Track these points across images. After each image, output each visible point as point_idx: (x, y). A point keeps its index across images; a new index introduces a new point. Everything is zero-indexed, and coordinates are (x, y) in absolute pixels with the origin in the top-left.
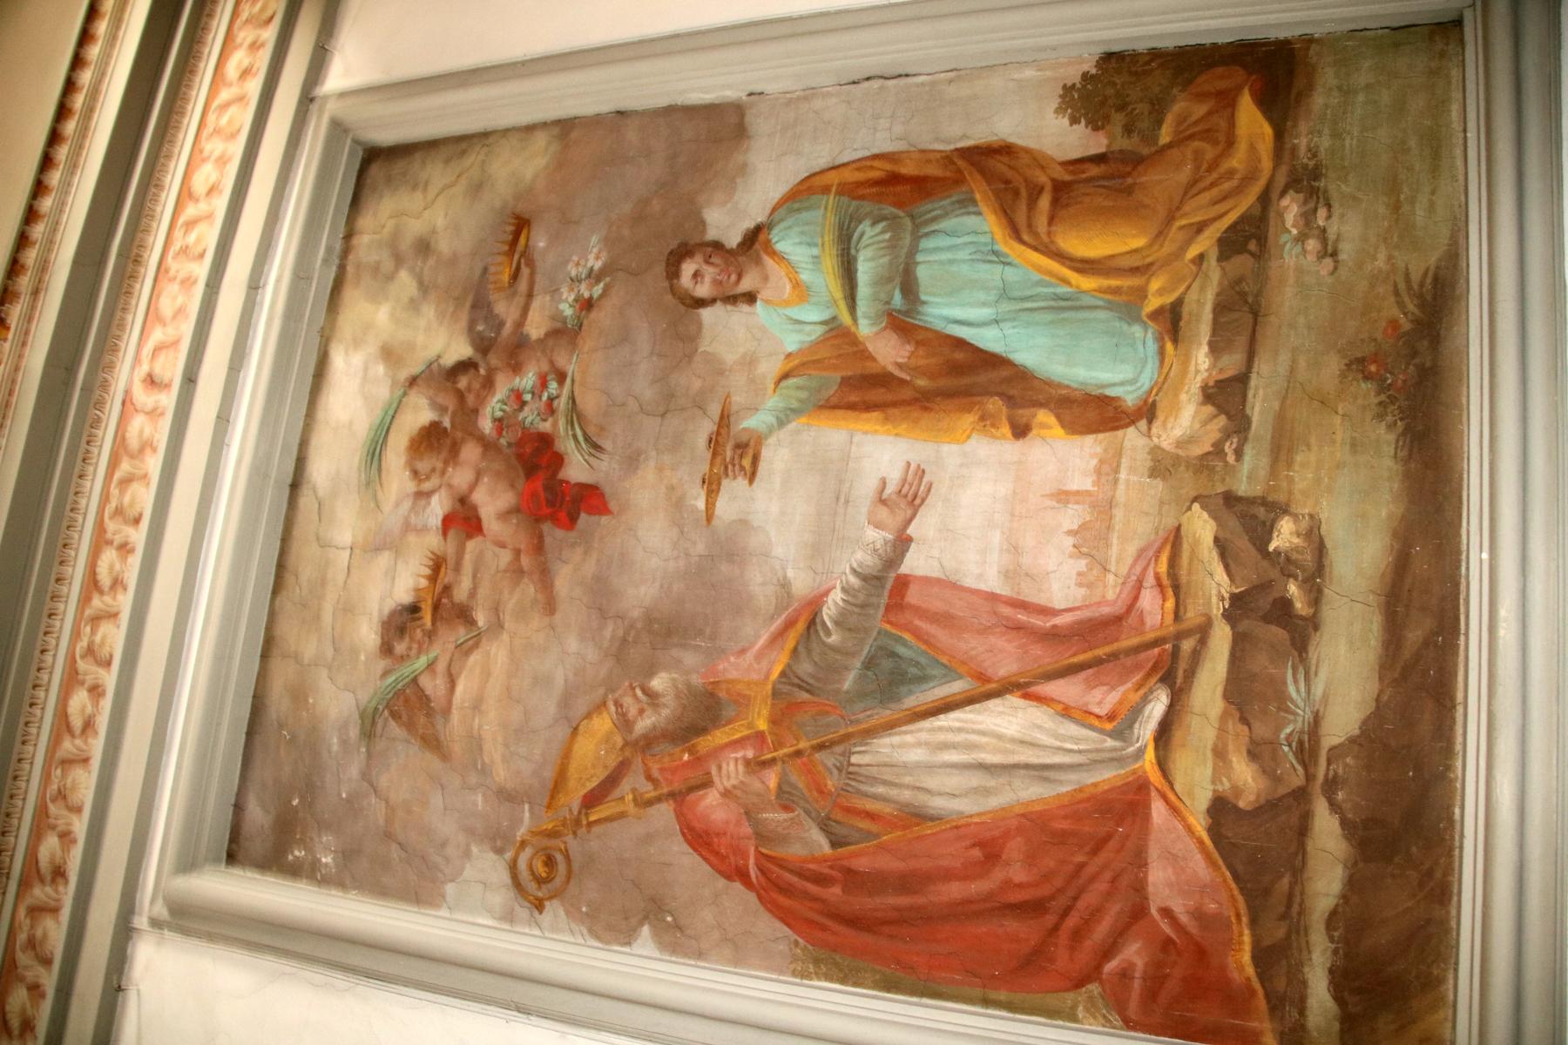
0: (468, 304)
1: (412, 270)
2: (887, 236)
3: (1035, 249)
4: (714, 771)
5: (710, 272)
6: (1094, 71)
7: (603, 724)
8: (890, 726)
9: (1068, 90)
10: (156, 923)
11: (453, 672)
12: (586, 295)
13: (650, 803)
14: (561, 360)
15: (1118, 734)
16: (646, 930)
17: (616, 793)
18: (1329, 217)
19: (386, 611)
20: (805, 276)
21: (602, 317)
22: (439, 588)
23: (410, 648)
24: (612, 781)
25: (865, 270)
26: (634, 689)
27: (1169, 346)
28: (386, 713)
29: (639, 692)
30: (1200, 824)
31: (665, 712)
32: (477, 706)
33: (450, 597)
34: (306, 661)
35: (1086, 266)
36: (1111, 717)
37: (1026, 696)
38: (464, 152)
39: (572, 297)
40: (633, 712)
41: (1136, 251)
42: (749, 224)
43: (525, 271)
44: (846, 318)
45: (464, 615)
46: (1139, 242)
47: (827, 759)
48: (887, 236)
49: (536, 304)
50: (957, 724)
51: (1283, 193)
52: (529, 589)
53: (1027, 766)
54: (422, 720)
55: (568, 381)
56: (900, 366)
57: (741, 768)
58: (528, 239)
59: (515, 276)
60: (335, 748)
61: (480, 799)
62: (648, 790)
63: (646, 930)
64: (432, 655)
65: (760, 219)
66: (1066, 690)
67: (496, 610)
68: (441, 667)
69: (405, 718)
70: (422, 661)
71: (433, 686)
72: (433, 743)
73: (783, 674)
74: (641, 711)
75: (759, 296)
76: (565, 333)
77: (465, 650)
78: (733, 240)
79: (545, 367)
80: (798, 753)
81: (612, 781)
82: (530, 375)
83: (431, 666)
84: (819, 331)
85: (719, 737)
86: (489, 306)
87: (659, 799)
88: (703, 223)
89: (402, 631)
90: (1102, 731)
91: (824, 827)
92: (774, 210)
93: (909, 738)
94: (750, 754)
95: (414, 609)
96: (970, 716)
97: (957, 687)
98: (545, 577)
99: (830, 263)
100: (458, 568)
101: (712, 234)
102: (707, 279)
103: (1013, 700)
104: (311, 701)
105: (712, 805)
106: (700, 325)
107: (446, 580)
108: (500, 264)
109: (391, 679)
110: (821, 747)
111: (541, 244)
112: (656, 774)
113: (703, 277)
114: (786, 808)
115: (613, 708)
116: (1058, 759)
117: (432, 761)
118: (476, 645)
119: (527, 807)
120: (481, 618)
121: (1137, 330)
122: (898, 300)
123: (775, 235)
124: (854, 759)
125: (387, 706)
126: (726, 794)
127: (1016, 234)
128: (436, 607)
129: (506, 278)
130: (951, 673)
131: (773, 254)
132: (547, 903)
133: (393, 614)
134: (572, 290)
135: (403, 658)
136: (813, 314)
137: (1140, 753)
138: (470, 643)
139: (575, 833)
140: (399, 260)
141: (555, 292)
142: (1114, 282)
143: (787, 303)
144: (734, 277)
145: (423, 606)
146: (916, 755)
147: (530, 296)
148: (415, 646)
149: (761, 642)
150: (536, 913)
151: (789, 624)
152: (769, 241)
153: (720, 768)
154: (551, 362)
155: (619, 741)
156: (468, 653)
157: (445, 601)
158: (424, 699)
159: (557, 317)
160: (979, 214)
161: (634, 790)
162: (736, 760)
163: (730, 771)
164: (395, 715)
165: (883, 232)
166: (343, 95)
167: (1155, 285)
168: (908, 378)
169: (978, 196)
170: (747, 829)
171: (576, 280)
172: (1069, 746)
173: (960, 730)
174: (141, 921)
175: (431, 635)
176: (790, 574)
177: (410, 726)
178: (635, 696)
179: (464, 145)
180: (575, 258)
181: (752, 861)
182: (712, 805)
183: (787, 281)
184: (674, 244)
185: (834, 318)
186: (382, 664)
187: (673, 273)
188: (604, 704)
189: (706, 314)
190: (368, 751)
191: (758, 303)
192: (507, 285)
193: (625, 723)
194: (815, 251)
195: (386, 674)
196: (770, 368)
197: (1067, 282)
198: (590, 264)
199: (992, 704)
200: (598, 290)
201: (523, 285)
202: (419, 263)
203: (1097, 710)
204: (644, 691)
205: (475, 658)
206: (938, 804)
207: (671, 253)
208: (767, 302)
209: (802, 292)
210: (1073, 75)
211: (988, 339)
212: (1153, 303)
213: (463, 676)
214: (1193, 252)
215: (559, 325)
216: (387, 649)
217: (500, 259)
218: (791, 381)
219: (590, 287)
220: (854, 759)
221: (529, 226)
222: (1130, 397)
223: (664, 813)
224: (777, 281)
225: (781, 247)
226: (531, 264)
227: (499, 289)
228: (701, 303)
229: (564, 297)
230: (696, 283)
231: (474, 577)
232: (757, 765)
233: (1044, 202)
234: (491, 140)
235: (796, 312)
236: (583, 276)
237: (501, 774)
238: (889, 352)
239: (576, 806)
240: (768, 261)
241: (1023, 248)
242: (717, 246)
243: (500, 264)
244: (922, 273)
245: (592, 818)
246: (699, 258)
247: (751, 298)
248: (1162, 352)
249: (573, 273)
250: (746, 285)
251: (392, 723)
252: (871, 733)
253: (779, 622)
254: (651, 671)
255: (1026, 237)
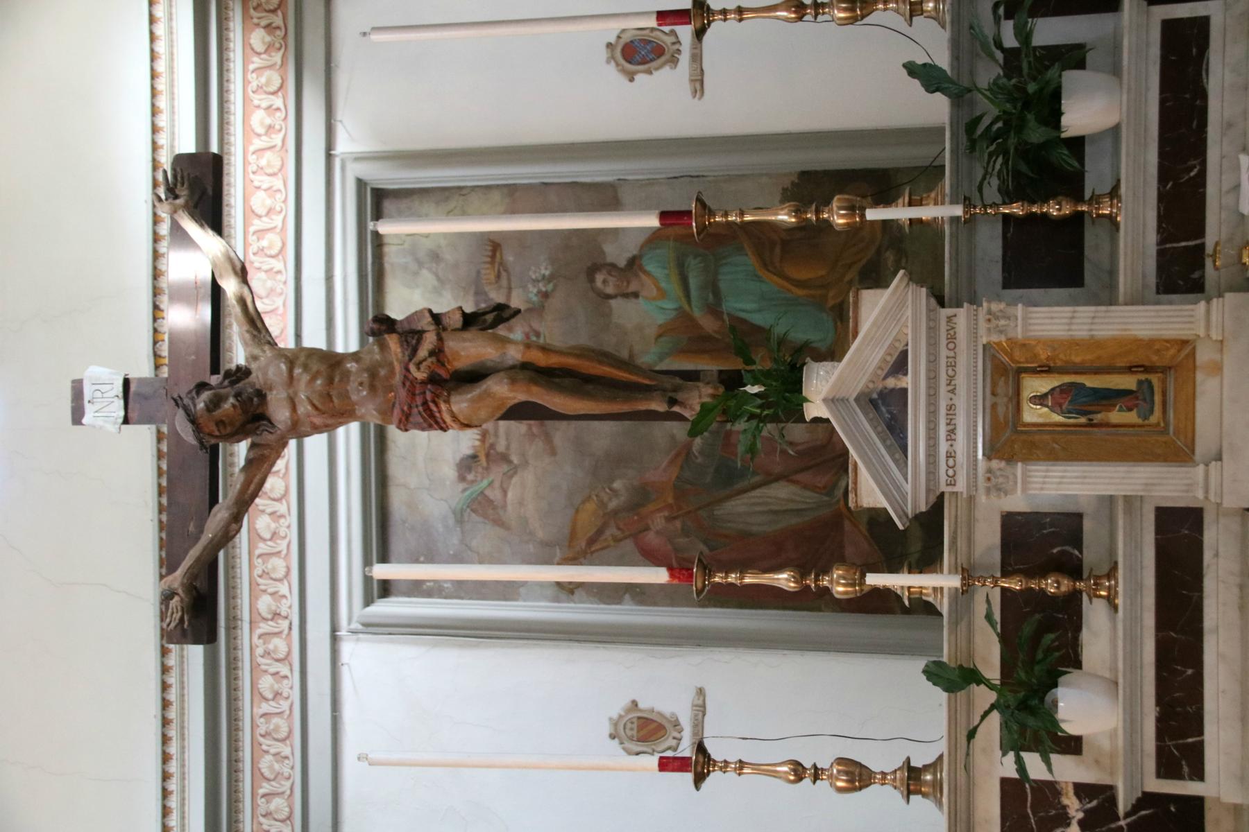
0: (472, 292)
1: (430, 270)
2: (702, 265)
3: (775, 274)
4: (650, 522)
5: (612, 280)
6: (796, 181)
7: (590, 506)
8: (729, 497)
9: (785, 190)
10: (354, 632)
11: (505, 486)
12: (544, 289)
13: (621, 540)
14: (536, 325)
15: (827, 495)
16: (627, 596)
17: (603, 538)
18: (907, 262)
19: (458, 459)
20: (663, 285)
21: (555, 303)
22: (487, 445)
23: (476, 476)
24: (600, 532)
25: (693, 283)
26: (604, 488)
27: (839, 324)
28: (468, 510)
29: (608, 490)
30: (863, 528)
31: (622, 499)
32: (521, 503)
33: (494, 449)
34: (412, 487)
35: (800, 284)
36: (824, 488)
37: (788, 481)
38: (447, 199)
39: (535, 291)
40: (606, 499)
41: (822, 276)
42: (629, 255)
43: (504, 274)
44: (686, 307)
45: (505, 458)
46: (822, 272)
47: (703, 513)
48: (702, 265)
49: (515, 294)
50: (759, 495)
51: (887, 249)
52: (539, 444)
53: (792, 510)
54: (490, 512)
55: (542, 336)
56: (715, 332)
57: (663, 521)
58: (501, 254)
59: (498, 276)
60: (441, 530)
61: (531, 546)
62: (618, 534)
63: (627, 596)
64: (490, 479)
65: (635, 252)
66: (804, 477)
67: (523, 455)
68: (497, 484)
69: (480, 511)
70: (485, 483)
71: (495, 494)
72: (499, 522)
73: (678, 477)
74: (610, 499)
75: (641, 294)
76: (537, 310)
77: (509, 476)
78: (622, 263)
79: (527, 329)
80: (689, 512)
81: (600, 532)
82: (519, 332)
83: (490, 484)
84: (674, 313)
85: (651, 507)
86: (486, 294)
87: (625, 538)
88: (603, 252)
89: (469, 469)
90: (821, 494)
91: (705, 543)
92: (642, 247)
93: (738, 502)
94: (666, 514)
95: (474, 457)
96: (765, 491)
97: (757, 479)
98: (548, 439)
99: (675, 278)
100: (496, 435)
101: (609, 259)
102: (611, 284)
103: (782, 483)
104: (420, 507)
105: (651, 538)
106: (610, 308)
107: (491, 441)
108: (488, 269)
109: (467, 493)
110: (699, 508)
111: (511, 259)
112: (621, 526)
113: (608, 282)
114: (688, 537)
115: (595, 498)
116: (803, 506)
117: (500, 531)
118: (515, 473)
119: (557, 547)
120: (515, 459)
121: (824, 316)
122: (711, 296)
123: (645, 262)
124: (715, 513)
125: (468, 507)
126: (658, 533)
127: (765, 265)
128: (488, 455)
129: (492, 277)
130: (755, 473)
131: (645, 272)
132: (576, 591)
133: (462, 460)
134: (535, 286)
135: (473, 482)
136: (669, 305)
137: (838, 501)
138: (511, 472)
139: (585, 558)
140: (420, 264)
141: (524, 287)
142: (812, 292)
143: (654, 299)
144: (625, 284)
145: (479, 454)
146: (742, 509)
147: (510, 289)
148: (479, 475)
149: (664, 465)
150: (571, 596)
151: (677, 455)
152: (641, 265)
153: (653, 521)
154: (531, 327)
155: (601, 513)
156: (511, 477)
157: (492, 451)
158: (490, 502)
159: (529, 301)
160: (747, 255)
161: (612, 535)
162: (661, 517)
163: (658, 522)
164: (473, 511)
165: (700, 263)
166: (360, 158)
167: (831, 294)
168: (720, 337)
169: (745, 245)
170: (669, 547)
171: (536, 281)
172: (808, 500)
173: (761, 497)
174: (342, 633)
175: (487, 469)
176: (675, 431)
177: (485, 516)
178: (606, 492)
179: (447, 194)
180: (533, 268)
181: (674, 560)
182: (651, 538)
183: (653, 286)
184: (589, 264)
185: (681, 308)
186: (461, 486)
187: (592, 280)
188: (590, 497)
189: (613, 302)
190: (463, 532)
191: (640, 298)
192: (494, 281)
193: (602, 504)
194: (666, 272)
195: (464, 490)
196: (651, 332)
197: (789, 290)
198: (543, 271)
199: (774, 485)
200: (550, 287)
201: (504, 282)
202: (434, 265)
203: (819, 485)
204: (611, 489)
205: (515, 480)
206: (755, 529)
207: (588, 268)
208: (646, 298)
209: (662, 294)
210: (787, 184)
211: (758, 319)
212: (831, 303)
213: (510, 489)
214: (847, 278)
215: (531, 306)
216: (462, 478)
217: (487, 266)
218: (663, 339)
219: (545, 286)
220: (715, 513)
221: (501, 249)
222: (823, 347)
223: (629, 545)
224: (649, 290)
225: (649, 268)
226: (506, 270)
227: (490, 284)
228: (609, 297)
229: (531, 289)
230: (605, 286)
231: (507, 439)
232: (669, 519)
233: (778, 250)
234: (464, 192)
235: (660, 303)
236: (540, 278)
237: (540, 534)
238: (709, 324)
239: (583, 544)
240: (643, 277)
241: (769, 274)
242: (613, 266)
243: (488, 269)
244: (723, 286)
245: (593, 549)
246: (604, 272)
247: (636, 295)
248: (836, 328)
249: (534, 277)
250: (633, 287)
251: (473, 515)
252: (721, 501)
253: (673, 453)
254: (612, 480)
255: (770, 268)
